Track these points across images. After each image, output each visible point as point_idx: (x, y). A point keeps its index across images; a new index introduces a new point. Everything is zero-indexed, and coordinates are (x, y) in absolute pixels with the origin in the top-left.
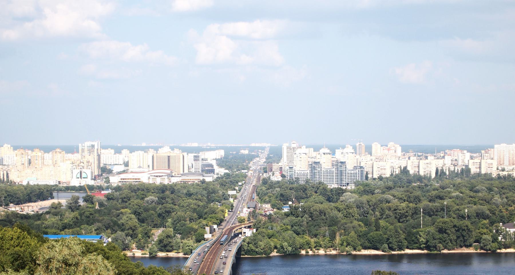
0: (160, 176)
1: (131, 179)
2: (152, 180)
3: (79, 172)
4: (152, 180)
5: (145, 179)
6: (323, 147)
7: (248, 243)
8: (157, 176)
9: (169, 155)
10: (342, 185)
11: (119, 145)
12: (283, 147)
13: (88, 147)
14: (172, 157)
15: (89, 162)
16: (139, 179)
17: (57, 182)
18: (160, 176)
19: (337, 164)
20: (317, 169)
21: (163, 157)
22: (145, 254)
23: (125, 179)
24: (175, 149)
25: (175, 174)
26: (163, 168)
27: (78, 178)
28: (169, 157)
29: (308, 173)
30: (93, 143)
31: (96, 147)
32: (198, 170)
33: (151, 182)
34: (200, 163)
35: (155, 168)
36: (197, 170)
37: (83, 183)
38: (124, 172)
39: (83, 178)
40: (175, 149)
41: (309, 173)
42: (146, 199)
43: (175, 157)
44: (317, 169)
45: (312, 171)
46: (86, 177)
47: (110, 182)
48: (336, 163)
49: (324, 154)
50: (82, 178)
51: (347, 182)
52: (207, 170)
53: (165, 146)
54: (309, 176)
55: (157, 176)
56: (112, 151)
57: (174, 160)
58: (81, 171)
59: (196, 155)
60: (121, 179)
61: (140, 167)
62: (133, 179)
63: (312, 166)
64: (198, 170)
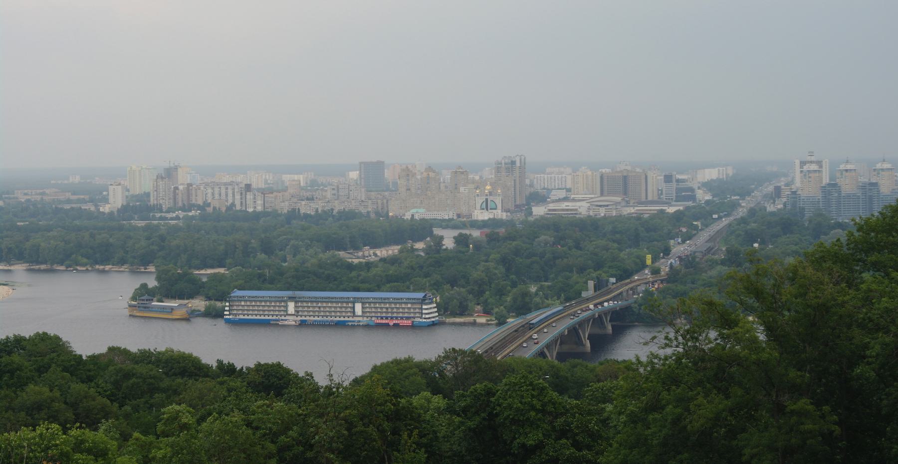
1: (563, 210)
3: (484, 202)
5: (583, 209)
7: (640, 305)
13: (505, 164)
16: (576, 210)
17: (455, 215)
20: (832, 194)
22: (491, 320)
27: (484, 209)
29: (819, 199)
33: (591, 213)
39: (491, 209)
44: (832, 194)
45: (825, 197)
46: (495, 207)
49: (847, 170)
50: (489, 209)
54: (821, 205)
55: (600, 206)
58: (487, 199)
60: (550, 210)
62: (567, 210)
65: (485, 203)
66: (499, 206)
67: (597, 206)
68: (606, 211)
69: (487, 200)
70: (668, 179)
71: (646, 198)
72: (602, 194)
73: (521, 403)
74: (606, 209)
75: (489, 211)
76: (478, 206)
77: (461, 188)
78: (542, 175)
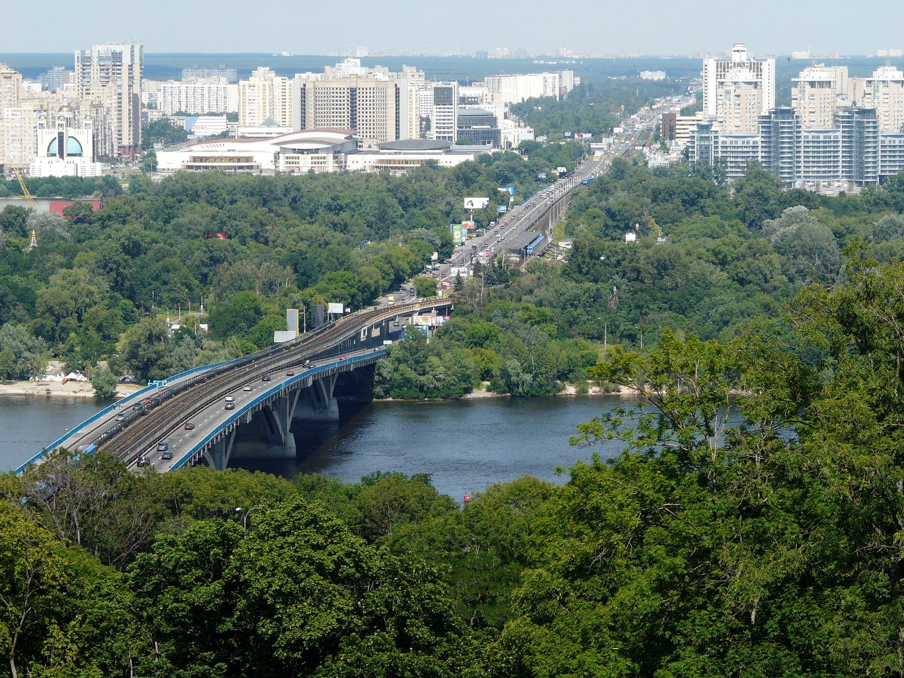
0: (309, 151)
1: (221, 159)
2: (287, 163)
4: (287, 163)
6: (883, 64)
8: (301, 151)
9: (354, 85)
10: (864, 181)
11: (285, 54)
12: (705, 63)
14: (365, 91)
15: (100, 105)
16: (248, 159)
18: (309, 151)
19: (848, 117)
21: (335, 90)
23: (206, 159)
24: (404, 66)
25: (370, 147)
26: (335, 126)
27: (54, 155)
28: (353, 91)
29: (756, 142)
30: (118, 49)
31: (126, 60)
32: (448, 133)
33: (282, 166)
34: (455, 110)
35: (310, 124)
36: (444, 133)
37: (60, 169)
38: (224, 136)
39: (69, 155)
40: (404, 66)
41: (760, 144)
42: (173, 222)
43: (372, 91)
47: (158, 167)
48: (847, 114)
49: (812, 84)
50: (65, 155)
51: (880, 173)
52: (476, 132)
53: (347, 57)
55: (301, 151)
56: (231, 73)
57: (368, 103)
59: (440, 84)
60: (195, 159)
61: (269, 123)
62: (231, 159)
63: (770, 122)
64: (448, 133)
65: (57, 141)
66: (88, 151)
67: (294, 151)
69: (61, 136)
70: (443, 97)
71: (397, 137)
72: (303, 127)
73: (743, 428)
75: (67, 159)
76: (43, 150)
77: (5, 110)
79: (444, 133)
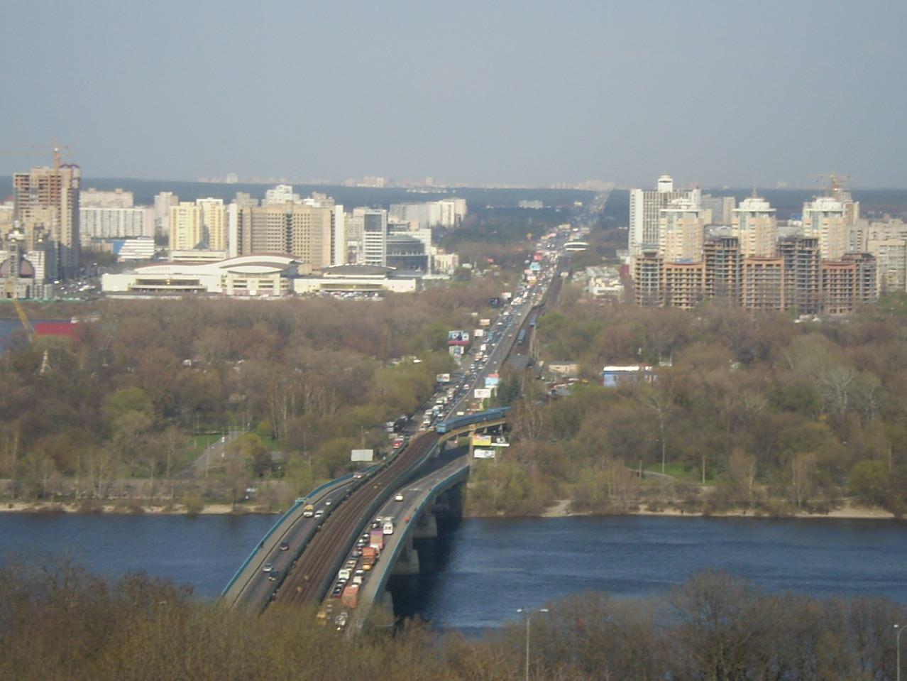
9: (289, 211)
12: (632, 193)
15: (42, 228)
16: (195, 282)
24: (314, 193)
28: (289, 216)
32: (378, 258)
35: (247, 248)
36: (374, 258)
40: (314, 193)
53: (278, 185)
56: (128, 197)
59: (371, 212)
64: (378, 258)
68: (260, 287)
71: (332, 262)
72: (241, 253)
74: (261, 282)
78: (115, 209)
79: (374, 258)
